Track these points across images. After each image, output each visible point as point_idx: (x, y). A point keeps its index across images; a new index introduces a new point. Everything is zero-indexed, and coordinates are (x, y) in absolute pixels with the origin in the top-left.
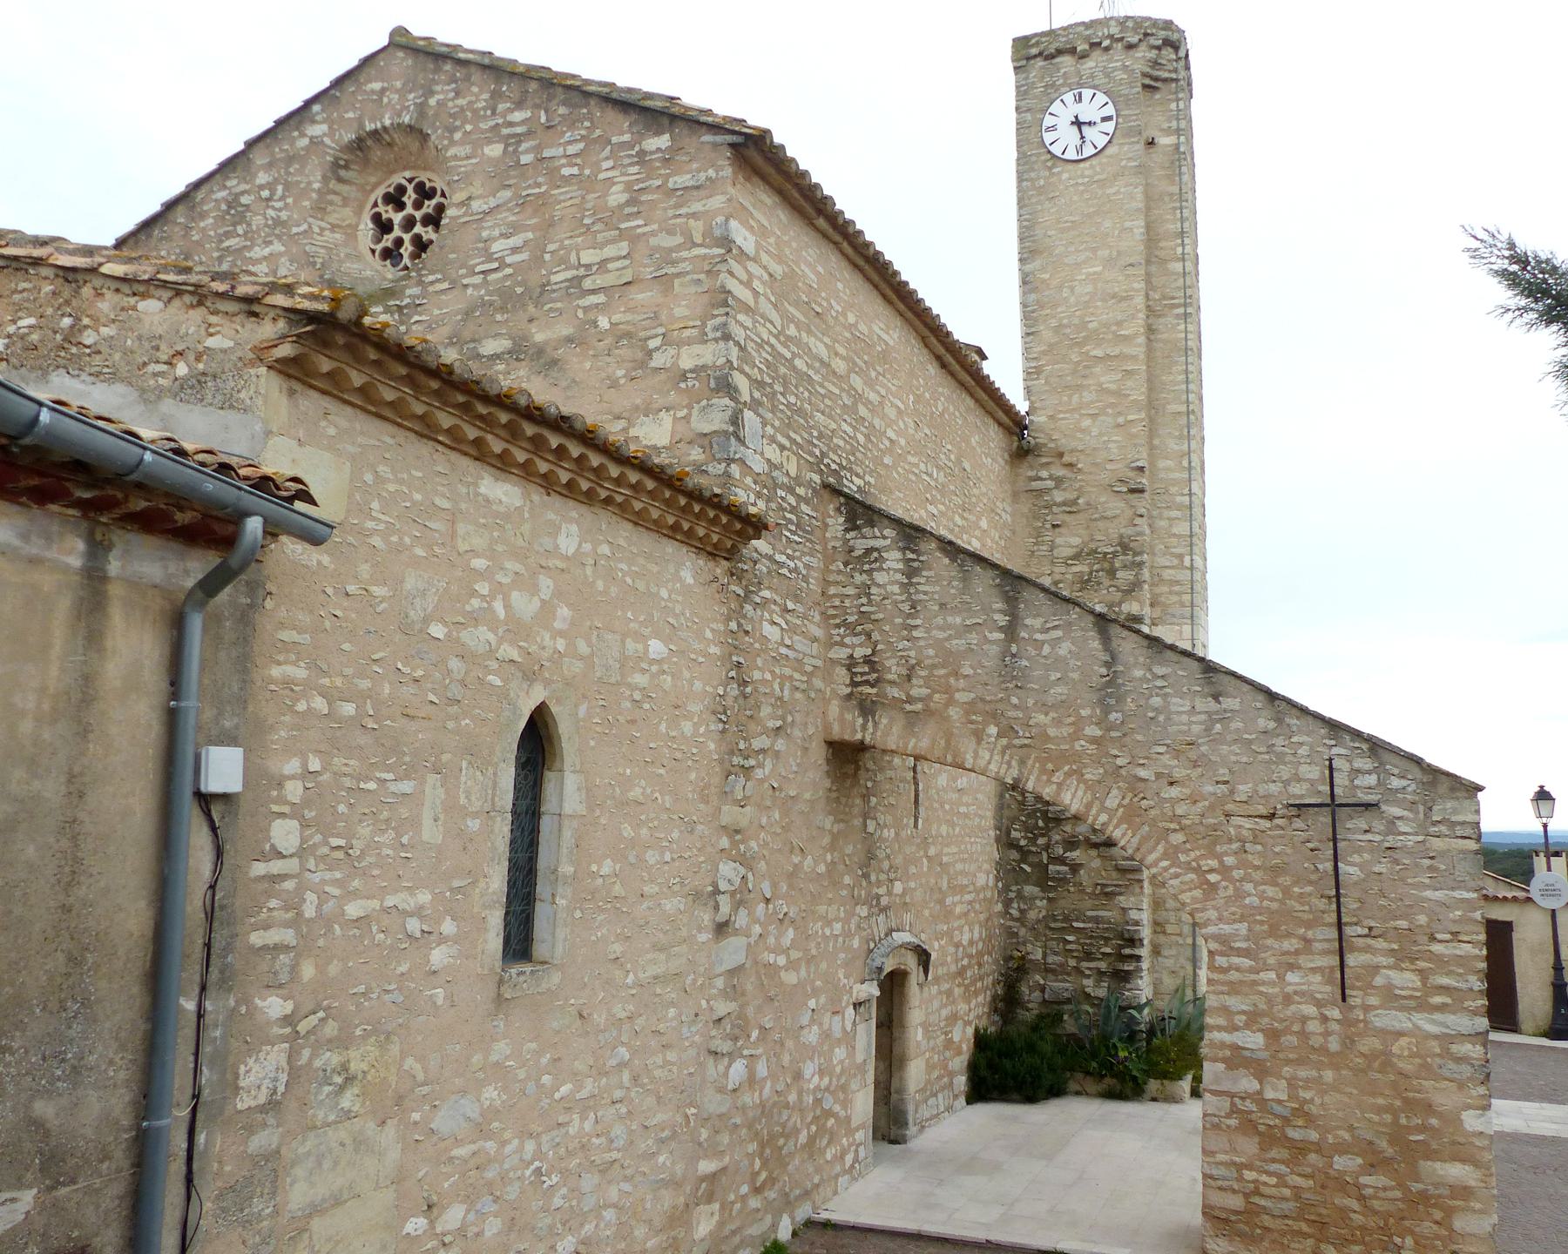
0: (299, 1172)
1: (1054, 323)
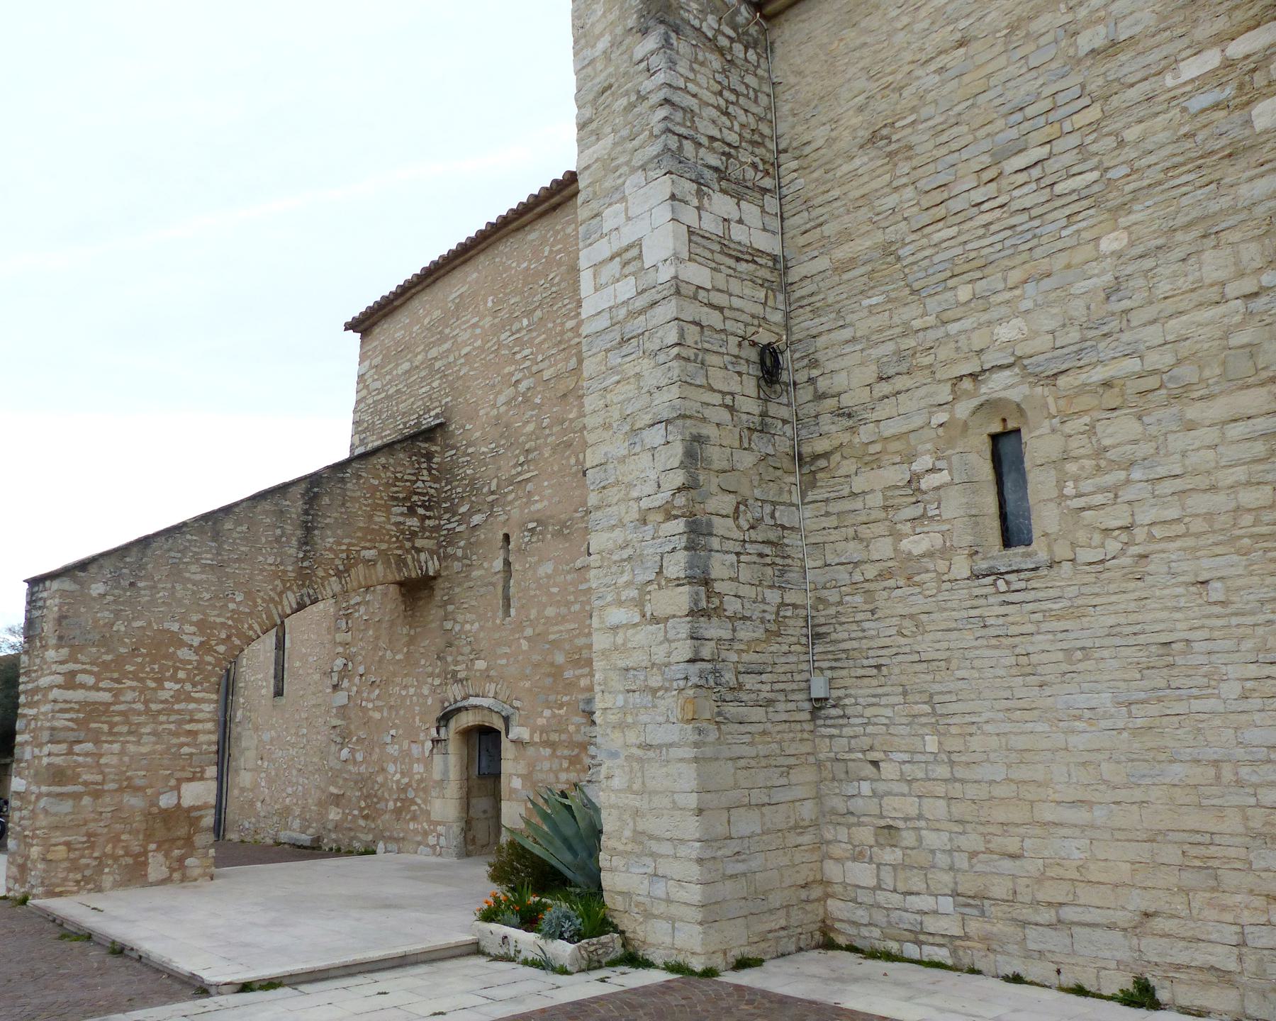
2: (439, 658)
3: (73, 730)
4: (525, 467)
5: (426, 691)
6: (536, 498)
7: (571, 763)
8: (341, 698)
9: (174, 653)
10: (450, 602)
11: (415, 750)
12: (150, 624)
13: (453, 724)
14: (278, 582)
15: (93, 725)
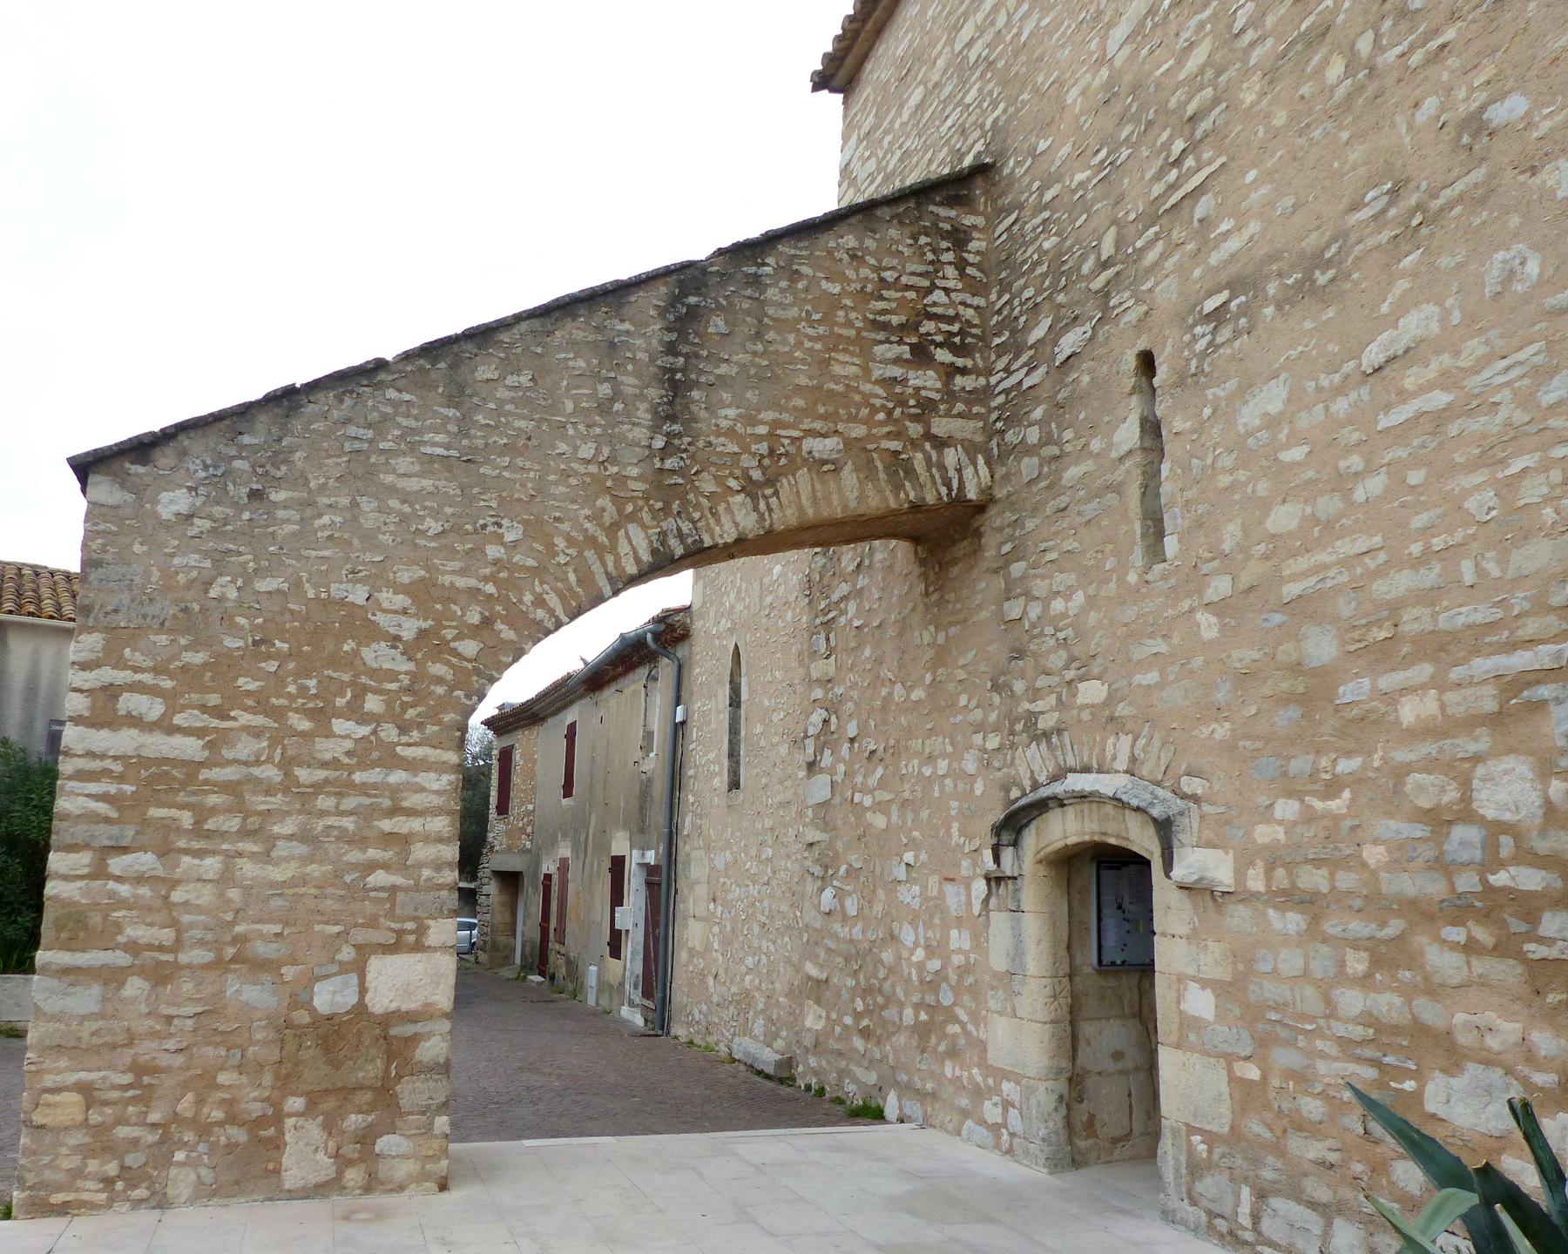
2: (996, 687)
3: (107, 820)
4: (1190, 162)
5: (970, 766)
6: (1224, 227)
7: (1377, 962)
8: (819, 789)
9: (356, 653)
10: (1017, 554)
12: (297, 584)
13: (1032, 840)
14: (604, 501)
15: (156, 812)
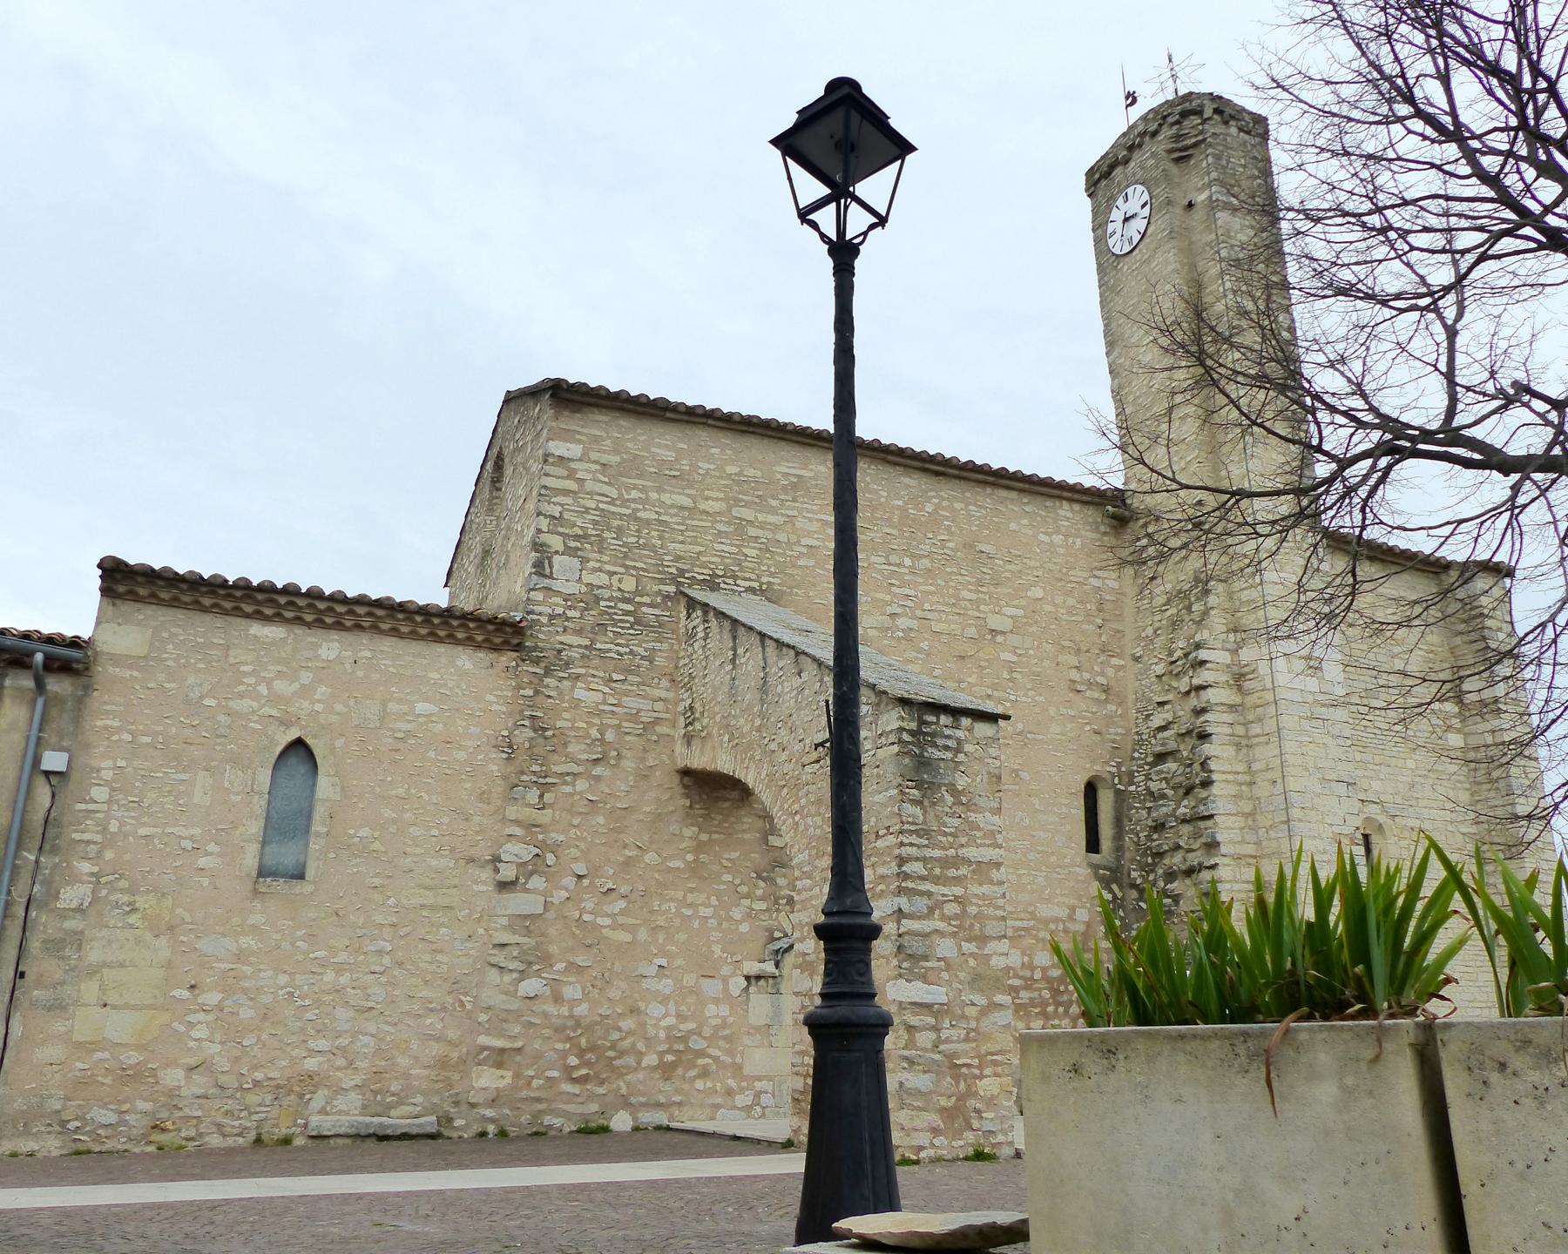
0: (95, 944)
1: (1131, 398)
2: (759, 877)
5: (737, 914)
11: (711, 987)
